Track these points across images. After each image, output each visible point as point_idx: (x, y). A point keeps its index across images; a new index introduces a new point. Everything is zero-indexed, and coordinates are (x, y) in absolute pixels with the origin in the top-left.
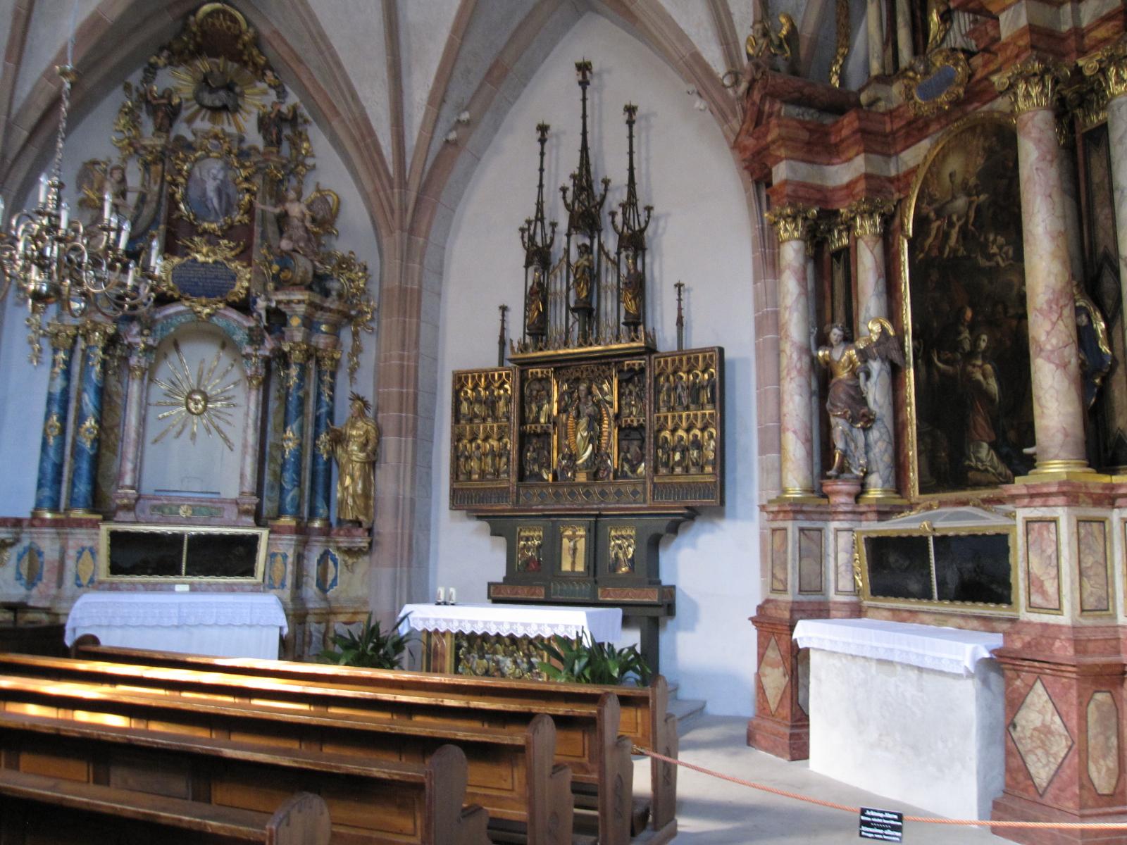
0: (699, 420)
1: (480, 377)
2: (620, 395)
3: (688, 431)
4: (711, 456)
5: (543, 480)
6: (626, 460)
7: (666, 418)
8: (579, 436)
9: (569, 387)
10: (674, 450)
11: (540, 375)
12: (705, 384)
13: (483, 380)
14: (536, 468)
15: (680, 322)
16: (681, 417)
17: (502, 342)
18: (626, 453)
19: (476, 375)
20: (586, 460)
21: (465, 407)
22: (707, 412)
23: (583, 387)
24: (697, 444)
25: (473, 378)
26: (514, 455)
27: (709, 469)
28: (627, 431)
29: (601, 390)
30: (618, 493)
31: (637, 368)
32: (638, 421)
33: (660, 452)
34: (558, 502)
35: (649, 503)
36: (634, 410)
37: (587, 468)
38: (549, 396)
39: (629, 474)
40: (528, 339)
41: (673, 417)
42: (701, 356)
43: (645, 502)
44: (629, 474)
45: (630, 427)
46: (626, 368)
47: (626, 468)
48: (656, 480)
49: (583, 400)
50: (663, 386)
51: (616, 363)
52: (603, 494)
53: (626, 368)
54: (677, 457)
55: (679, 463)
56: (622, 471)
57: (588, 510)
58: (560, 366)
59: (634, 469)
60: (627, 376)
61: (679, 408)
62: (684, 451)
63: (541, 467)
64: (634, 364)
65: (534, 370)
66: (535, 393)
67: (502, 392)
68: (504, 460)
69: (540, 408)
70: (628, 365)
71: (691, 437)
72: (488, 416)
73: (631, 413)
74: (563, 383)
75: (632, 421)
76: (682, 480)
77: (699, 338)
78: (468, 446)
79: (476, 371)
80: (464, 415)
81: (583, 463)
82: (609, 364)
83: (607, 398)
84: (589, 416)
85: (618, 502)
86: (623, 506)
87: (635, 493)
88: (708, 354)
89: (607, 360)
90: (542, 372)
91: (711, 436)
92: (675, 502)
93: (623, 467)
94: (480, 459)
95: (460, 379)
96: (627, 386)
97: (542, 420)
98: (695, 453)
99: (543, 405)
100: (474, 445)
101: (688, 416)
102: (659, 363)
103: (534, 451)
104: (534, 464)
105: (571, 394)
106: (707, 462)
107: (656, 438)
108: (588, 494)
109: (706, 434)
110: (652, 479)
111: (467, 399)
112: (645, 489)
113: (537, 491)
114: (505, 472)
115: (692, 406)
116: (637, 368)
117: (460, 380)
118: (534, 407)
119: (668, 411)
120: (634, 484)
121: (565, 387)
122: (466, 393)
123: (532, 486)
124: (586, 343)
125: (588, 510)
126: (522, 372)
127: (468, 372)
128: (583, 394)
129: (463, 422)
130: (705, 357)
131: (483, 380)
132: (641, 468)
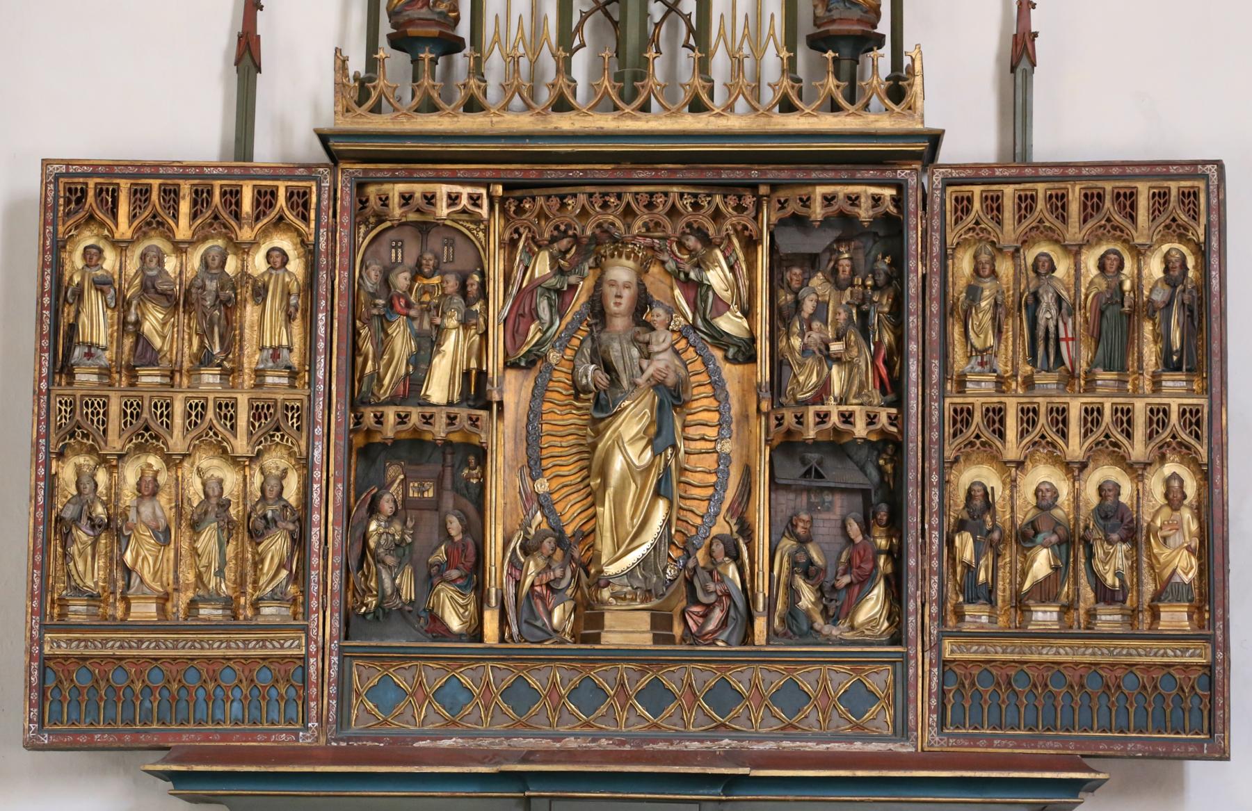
0: (1140, 431)
1: (171, 195)
2: (781, 318)
3: (1076, 470)
4: (1185, 567)
5: (446, 634)
6: (809, 571)
7: (996, 417)
8: (618, 464)
9: (560, 271)
10: (1026, 537)
11: (443, 210)
12: (1160, 297)
13: (185, 207)
14: (407, 586)
15: (1021, 52)
16: (1060, 418)
17: (248, 53)
18: (803, 541)
19: (152, 191)
20: (643, 562)
21: (96, 322)
22: (1174, 405)
23: (621, 272)
24: (1117, 520)
25: (140, 195)
26: (326, 530)
27: (1175, 617)
28: (813, 457)
29: (697, 290)
30: (792, 697)
31: (864, 213)
32: (871, 419)
33: (966, 546)
34: (523, 726)
35: (927, 737)
36: (837, 376)
37: (648, 594)
38: (472, 293)
39: (819, 622)
40: (395, 62)
41: (1029, 416)
42: (1144, 190)
43: (902, 730)
44: (819, 622)
45: (838, 445)
46: (818, 211)
47: (807, 597)
48: (949, 649)
49: (620, 323)
50: (973, 293)
51: (774, 187)
52: (723, 697)
53: (818, 211)
54: (1042, 563)
55: (1045, 592)
56: (792, 612)
57: (655, 758)
58: (527, 178)
59: (838, 604)
60: (817, 243)
61: (1048, 381)
62: (1072, 543)
63: (429, 580)
64: (854, 200)
65: (418, 189)
66: (401, 280)
67: (258, 263)
68: (277, 546)
69: (429, 344)
70: (828, 200)
71: (1091, 495)
72: (204, 359)
73: (823, 391)
74: (536, 244)
75: (847, 418)
76: (1063, 653)
77: (1082, 122)
78: (102, 477)
79: (154, 169)
80: (91, 350)
81: (630, 573)
82: (754, 187)
83: (731, 323)
84: (658, 385)
85: (788, 730)
86: (812, 746)
87: (858, 698)
88: (1173, 186)
89: (735, 174)
90: (453, 199)
91: (1174, 498)
92: (1032, 741)
93: (793, 594)
94: (163, 536)
95: (77, 196)
96: (805, 283)
97: (438, 389)
98: (1113, 561)
99: (440, 330)
100: (131, 473)
101: (1092, 416)
102: (964, 205)
103: (390, 520)
104: (394, 571)
105: (561, 296)
106: (1167, 591)
107: (944, 483)
108: (656, 697)
109: (1155, 485)
110: (938, 647)
111: (101, 285)
112: (903, 683)
113: (433, 676)
114: (277, 597)
115: (1105, 377)
116: (864, 213)
117: (78, 194)
118: (401, 342)
119: (1001, 384)
120: (858, 663)
121: (542, 266)
122: (93, 256)
123: (404, 656)
124: (628, 95)
125: (655, 758)
126: (361, 186)
127: (111, 170)
128: (620, 304)
129: (86, 377)
130: (1161, 198)
131: (185, 207)
132: (873, 606)
